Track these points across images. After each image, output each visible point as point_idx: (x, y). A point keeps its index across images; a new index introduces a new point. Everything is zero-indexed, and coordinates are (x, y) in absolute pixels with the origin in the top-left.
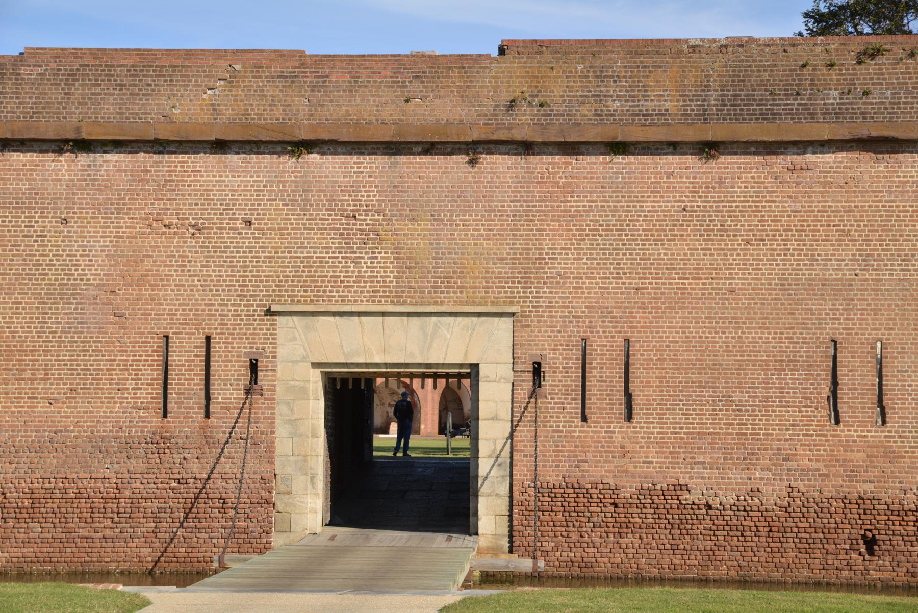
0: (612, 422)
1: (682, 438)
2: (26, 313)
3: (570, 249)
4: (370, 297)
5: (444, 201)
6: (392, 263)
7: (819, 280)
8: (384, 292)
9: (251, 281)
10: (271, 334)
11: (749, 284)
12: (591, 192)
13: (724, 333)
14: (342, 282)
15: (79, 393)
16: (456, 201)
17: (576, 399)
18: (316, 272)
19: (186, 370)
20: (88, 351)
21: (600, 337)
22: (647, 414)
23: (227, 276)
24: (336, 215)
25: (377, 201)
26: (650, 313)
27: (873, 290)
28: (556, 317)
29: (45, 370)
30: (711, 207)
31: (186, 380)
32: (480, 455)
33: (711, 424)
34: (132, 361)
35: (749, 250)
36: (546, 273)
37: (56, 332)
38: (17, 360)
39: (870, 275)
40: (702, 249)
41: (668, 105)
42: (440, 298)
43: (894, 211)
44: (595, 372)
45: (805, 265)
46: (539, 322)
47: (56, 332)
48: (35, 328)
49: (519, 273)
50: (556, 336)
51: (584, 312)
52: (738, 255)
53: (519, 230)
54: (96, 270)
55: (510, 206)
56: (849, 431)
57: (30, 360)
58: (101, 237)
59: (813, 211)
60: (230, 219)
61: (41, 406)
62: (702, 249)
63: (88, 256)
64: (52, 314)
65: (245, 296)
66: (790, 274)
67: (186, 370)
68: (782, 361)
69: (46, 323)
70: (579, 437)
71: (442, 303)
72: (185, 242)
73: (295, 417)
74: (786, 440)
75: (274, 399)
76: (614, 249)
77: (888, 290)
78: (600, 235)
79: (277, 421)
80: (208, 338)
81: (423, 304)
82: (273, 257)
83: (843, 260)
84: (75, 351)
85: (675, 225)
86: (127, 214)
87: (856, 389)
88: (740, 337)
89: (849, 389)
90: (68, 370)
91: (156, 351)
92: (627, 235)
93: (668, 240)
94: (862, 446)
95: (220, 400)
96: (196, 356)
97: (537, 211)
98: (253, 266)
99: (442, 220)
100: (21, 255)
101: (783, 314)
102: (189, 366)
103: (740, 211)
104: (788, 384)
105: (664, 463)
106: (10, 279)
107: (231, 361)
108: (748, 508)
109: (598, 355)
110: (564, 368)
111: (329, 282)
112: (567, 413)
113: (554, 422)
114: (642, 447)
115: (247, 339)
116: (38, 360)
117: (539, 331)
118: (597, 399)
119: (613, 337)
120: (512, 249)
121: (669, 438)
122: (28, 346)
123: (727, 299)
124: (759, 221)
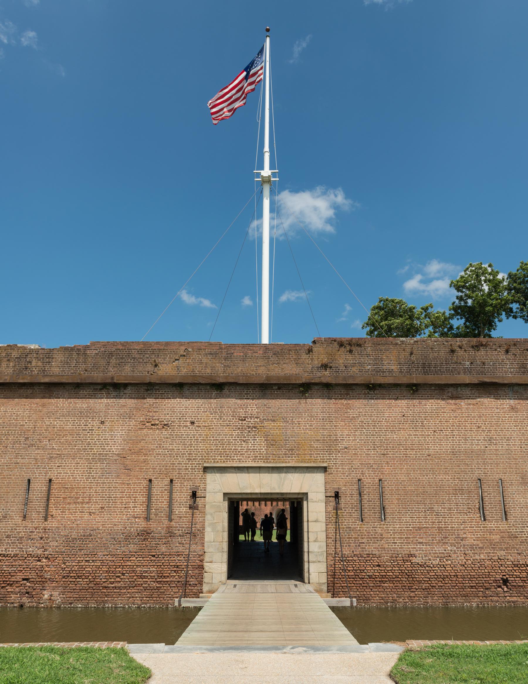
0: (376, 522)
1: (411, 530)
2: (81, 468)
3: (350, 435)
4: (253, 459)
5: (289, 412)
6: (264, 442)
7: (470, 450)
8: (260, 457)
9: (194, 452)
10: (203, 478)
11: (437, 452)
13: (427, 476)
14: (239, 452)
15: (105, 510)
16: (294, 412)
17: (357, 511)
18: (226, 447)
19: (160, 497)
20: (111, 488)
21: (367, 478)
22: (393, 518)
23: (182, 449)
24: (236, 419)
25: (256, 412)
26: (391, 466)
27: (495, 454)
29: (89, 497)
30: (416, 415)
31: (160, 502)
33: (424, 522)
34: (133, 492)
35: (435, 435)
36: (339, 447)
37: (95, 478)
38: (75, 492)
39: (493, 447)
40: (414, 435)
41: (393, 367)
43: (500, 417)
44: (366, 497)
45: (462, 442)
46: (337, 471)
47: (95, 478)
48: (85, 476)
49: (327, 447)
50: (346, 478)
51: (359, 466)
52: (431, 438)
53: (325, 426)
54: (117, 446)
56: (491, 524)
57: (82, 492)
58: (121, 430)
59: (464, 417)
60: (184, 421)
61: (86, 516)
62: (414, 435)
63: (114, 439)
64: (94, 469)
65: (191, 459)
66: (456, 447)
67: (160, 497)
68: (456, 490)
69: (91, 473)
70: (360, 530)
71: (289, 462)
72: (162, 433)
74: (461, 530)
75: (205, 512)
76: (372, 435)
77: (501, 454)
78: (365, 428)
79: (206, 524)
81: (280, 462)
82: (205, 440)
83: (480, 440)
84: (104, 488)
85: (400, 424)
86: (134, 419)
87: (492, 503)
88: (435, 478)
89: (489, 503)
90: (101, 497)
91: (145, 488)
92: (377, 428)
93: (397, 431)
94: (498, 533)
95: (177, 513)
96: (165, 490)
97: (334, 417)
98: (195, 444)
100: (81, 440)
101: (455, 466)
102: (162, 495)
103: (430, 417)
104: (459, 501)
105: (403, 543)
106: (75, 452)
107: (183, 492)
108: (445, 566)
110: (350, 494)
111: (233, 452)
112: (353, 518)
113: (347, 522)
114: (391, 535)
116: (86, 493)
117: (337, 476)
119: (374, 478)
120: (322, 435)
121: (404, 530)
122: (81, 485)
123: (427, 459)
124: (439, 422)
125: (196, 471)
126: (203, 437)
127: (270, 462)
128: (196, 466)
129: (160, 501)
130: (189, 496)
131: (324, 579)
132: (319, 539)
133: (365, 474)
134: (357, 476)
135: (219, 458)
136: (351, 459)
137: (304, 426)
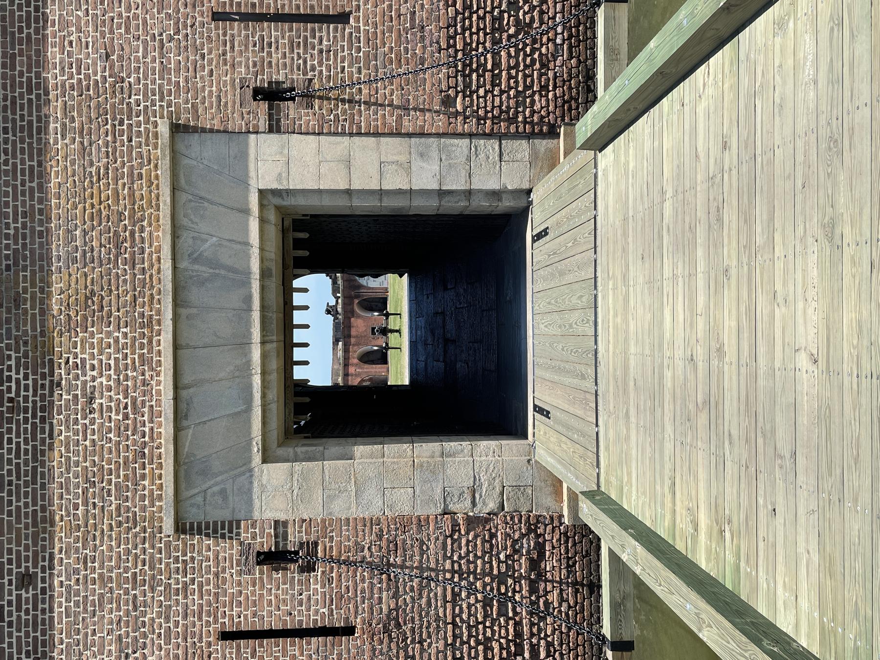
32: (406, 187)
42: (151, 254)
50: (210, 62)
51: (169, 16)
53: (30, 123)
60: (19, 609)
80: (226, 636)
99: (16, 251)
115: (224, 571)
125: (193, 559)
126: (77, 540)
127: (159, 313)
128: (177, 560)
130: (274, 575)
131: (521, 149)
132: (403, 158)
135: (146, 483)
137: (32, 198)
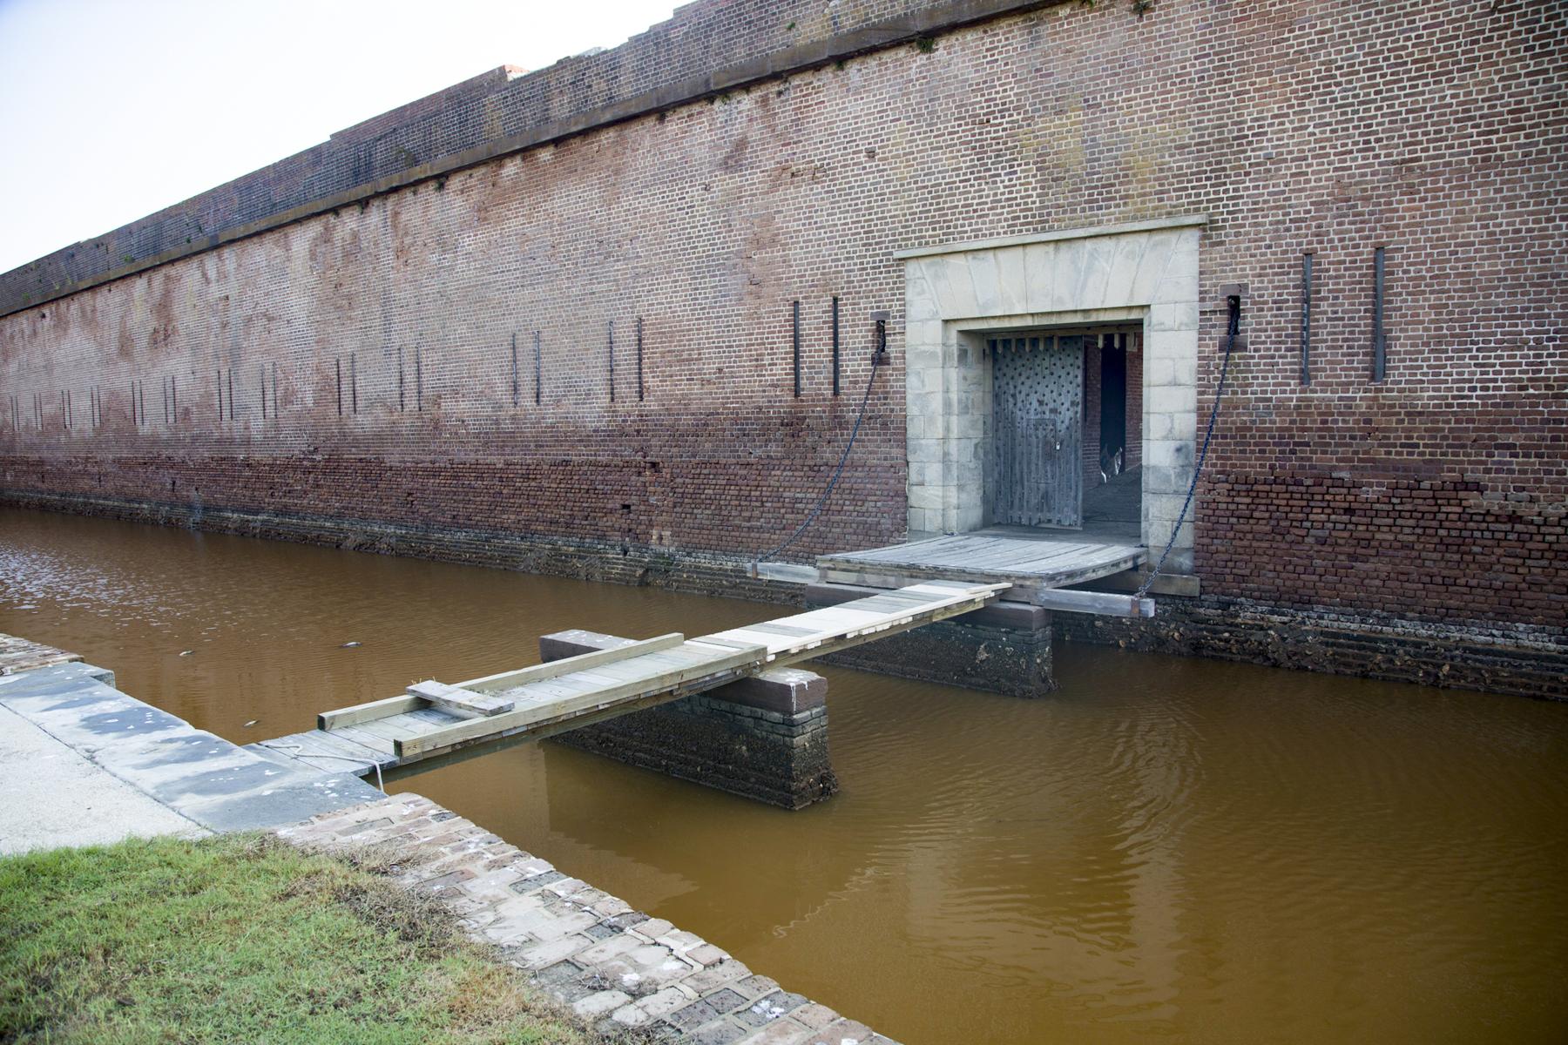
3: (1287, 115)
12: (1322, 17)
16: (1117, 74)
17: (1292, 349)
21: (1333, 248)
22: (1411, 367)
26: (1423, 199)
28: (1263, 224)
44: (1324, 306)
46: (1237, 234)
49: (1209, 164)
50: (1263, 255)
53: (1208, 99)
55: (1193, 65)
71: (1099, 223)
73: (927, 389)
78: (1338, 84)
79: (909, 397)
80: (835, 300)
99: (1099, 105)
109: (1330, 277)
110: (1275, 302)
118: (1328, 348)
119: (1357, 246)
127: (1052, 228)
129: (817, 352)
133: (1328, 233)
134: (1299, 244)
136: (1283, 192)
